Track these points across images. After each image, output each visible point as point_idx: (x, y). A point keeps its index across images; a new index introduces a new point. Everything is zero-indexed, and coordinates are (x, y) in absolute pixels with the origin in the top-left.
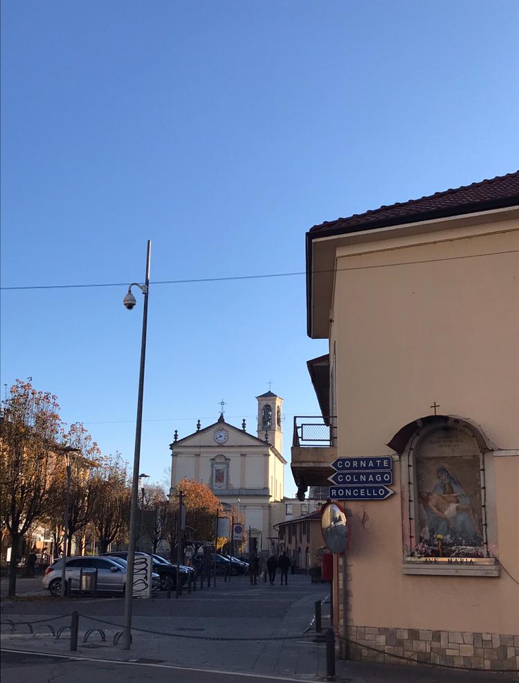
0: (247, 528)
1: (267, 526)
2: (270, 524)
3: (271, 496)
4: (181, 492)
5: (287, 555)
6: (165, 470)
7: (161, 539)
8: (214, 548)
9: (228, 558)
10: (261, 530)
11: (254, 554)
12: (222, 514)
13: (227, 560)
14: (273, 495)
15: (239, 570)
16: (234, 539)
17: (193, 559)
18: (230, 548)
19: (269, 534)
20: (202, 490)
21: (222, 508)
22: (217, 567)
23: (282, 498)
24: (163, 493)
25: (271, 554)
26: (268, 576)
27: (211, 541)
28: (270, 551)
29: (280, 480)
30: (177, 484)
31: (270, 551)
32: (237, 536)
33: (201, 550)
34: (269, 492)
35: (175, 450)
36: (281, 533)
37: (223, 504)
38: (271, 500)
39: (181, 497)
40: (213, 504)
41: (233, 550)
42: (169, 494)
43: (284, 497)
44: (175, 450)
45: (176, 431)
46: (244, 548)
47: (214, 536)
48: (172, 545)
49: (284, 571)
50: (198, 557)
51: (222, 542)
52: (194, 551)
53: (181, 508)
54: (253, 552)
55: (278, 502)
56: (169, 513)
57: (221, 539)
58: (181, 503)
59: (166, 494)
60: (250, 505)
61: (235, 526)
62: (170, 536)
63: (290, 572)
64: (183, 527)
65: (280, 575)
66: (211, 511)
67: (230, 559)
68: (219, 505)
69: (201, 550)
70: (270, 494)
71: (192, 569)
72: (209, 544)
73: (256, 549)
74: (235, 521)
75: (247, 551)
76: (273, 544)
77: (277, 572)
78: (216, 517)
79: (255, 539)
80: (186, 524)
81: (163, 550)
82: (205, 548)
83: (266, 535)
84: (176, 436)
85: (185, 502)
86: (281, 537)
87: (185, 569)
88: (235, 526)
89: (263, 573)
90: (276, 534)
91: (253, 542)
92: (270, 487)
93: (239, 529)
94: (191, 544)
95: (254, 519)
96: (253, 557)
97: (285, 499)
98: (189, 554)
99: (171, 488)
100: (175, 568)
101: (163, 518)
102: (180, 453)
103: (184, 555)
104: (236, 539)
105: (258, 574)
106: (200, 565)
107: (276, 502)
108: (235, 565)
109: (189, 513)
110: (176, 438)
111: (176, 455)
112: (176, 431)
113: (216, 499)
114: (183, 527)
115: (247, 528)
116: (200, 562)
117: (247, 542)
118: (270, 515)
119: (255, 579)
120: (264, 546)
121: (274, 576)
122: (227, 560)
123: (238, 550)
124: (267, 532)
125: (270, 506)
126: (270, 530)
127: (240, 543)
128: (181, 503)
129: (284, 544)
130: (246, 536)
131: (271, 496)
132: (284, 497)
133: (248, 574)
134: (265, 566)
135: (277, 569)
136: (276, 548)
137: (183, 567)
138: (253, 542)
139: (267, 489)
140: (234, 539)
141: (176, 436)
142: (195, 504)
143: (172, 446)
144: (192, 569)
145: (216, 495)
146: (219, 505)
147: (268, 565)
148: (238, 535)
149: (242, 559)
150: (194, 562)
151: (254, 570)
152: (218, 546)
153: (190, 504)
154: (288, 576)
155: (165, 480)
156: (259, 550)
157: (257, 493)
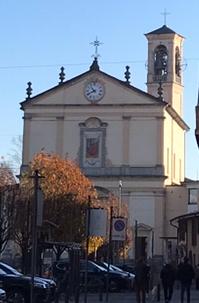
0: (131, 224)
1: (161, 219)
2: (165, 218)
3: (166, 177)
4: (37, 172)
5: (189, 262)
6: (14, 140)
7: (7, 239)
8: (85, 252)
9: (105, 267)
10: (152, 226)
11: (141, 261)
12: (95, 204)
13: (103, 269)
14: (169, 176)
15: (119, 285)
16: (113, 239)
17: (55, 268)
18: (108, 252)
19: (164, 232)
20: (67, 169)
21: (95, 194)
22: (89, 279)
23: (183, 180)
24: (10, 173)
25: (167, 261)
26: (162, 292)
27: (80, 242)
28: (166, 257)
29: (180, 155)
30: (31, 159)
31: (166, 257)
32: (118, 236)
33: (65, 255)
34: (163, 172)
35: (28, 111)
36: (182, 230)
37: (99, 189)
38: (167, 182)
39: (36, 178)
40: (83, 189)
41: (111, 254)
42: (18, 174)
43: (186, 179)
44: (28, 111)
45: (30, 84)
46: (128, 252)
47: (85, 235)
48: (24, 247)
49: (186, 286)
50: (61, 266)
51: (95, 244)
52: (55, 256)
53: (36, 193)
54: (140, 258)
55: (176, 185)
56: (20, 203)
57: (95, 239)
58: (37, 187)
59: (14, 175)
60: (136, 190)
61: (114, 220)
62: (20, 235)
63: (195, 286)
64: (40, 222)
65: (180, 291)
66: (81, 198)
67: (108, 269)
68: (92, 190)
69: (65, 255)
70: (166, 174)
71: (52, 282)
72: (76, 247)
73: (144, 254)
74: (115, 213)
75: (132, 257)
76: (170, 246)
77: (175, 286)
78: (87, 208)
79: (144, 239)
80: (44, 217)
81: (11, 255)
82: (71, 253)
83: (159, 234)
84: (29, 91)
85: (42, 185)
86: (181, 237)
87: (43, 282)
88: (114, 220)
89: (155, 288)
90: (173, 232)
91: (141, 244)
92: (165, 164)
93: (120, 225)
94: (51, 246)
95: (142, 211)
96: (141, 266)
97: (187, 181)
98: (48, 261)
99: (22, 166)
100: (28, 281)
101: (11, 208)
102: (35, 115)
103: (40, 262)
104: (117, 239)
105: (147, 289)
106: (65, 276)
107: (174, 185)
108: (115, 277)
109: (47, 203)
110: (29, 94)
111: (30, 118)
112: (30, 84)
113: (87, 182)
114: (40, 222)
115: (131, 224)
116: (64, 272)
117: (132, 244)
118: (165, 205)
119: (144, 296)
120: (156, 249)
121: (171, 292)
122: (103, 269)
123: (118, 255)
124: (161, 230)
125: (164, 192)
126: (165, 226)
127: (122, 245)
128: (37, 187)
129: (186, 247)
130: (131, 235)
131: (166, 177)
132: (186, 179)
133: (133, 290)
134: (158, 278)
135: (176, 282)
136: (174, 252)
137: (40, 280)
138: (141, 244)
139: (160, 167)
140: (113, 239)
141: (29, 91)
142: (56, 187)
143: (23, 105)
144: (52, 282)
145: (87, 176)
146: (92, 190)
147: (162, 277)
148: (120, 233)
149: (124, 268)
150: (56, 272)
151: (142, 284)
152: (90, 250)
153: (51, 189)
154: (191, 292)
155: (14, 153)
156: (150, 255)
157: (148, 173)
